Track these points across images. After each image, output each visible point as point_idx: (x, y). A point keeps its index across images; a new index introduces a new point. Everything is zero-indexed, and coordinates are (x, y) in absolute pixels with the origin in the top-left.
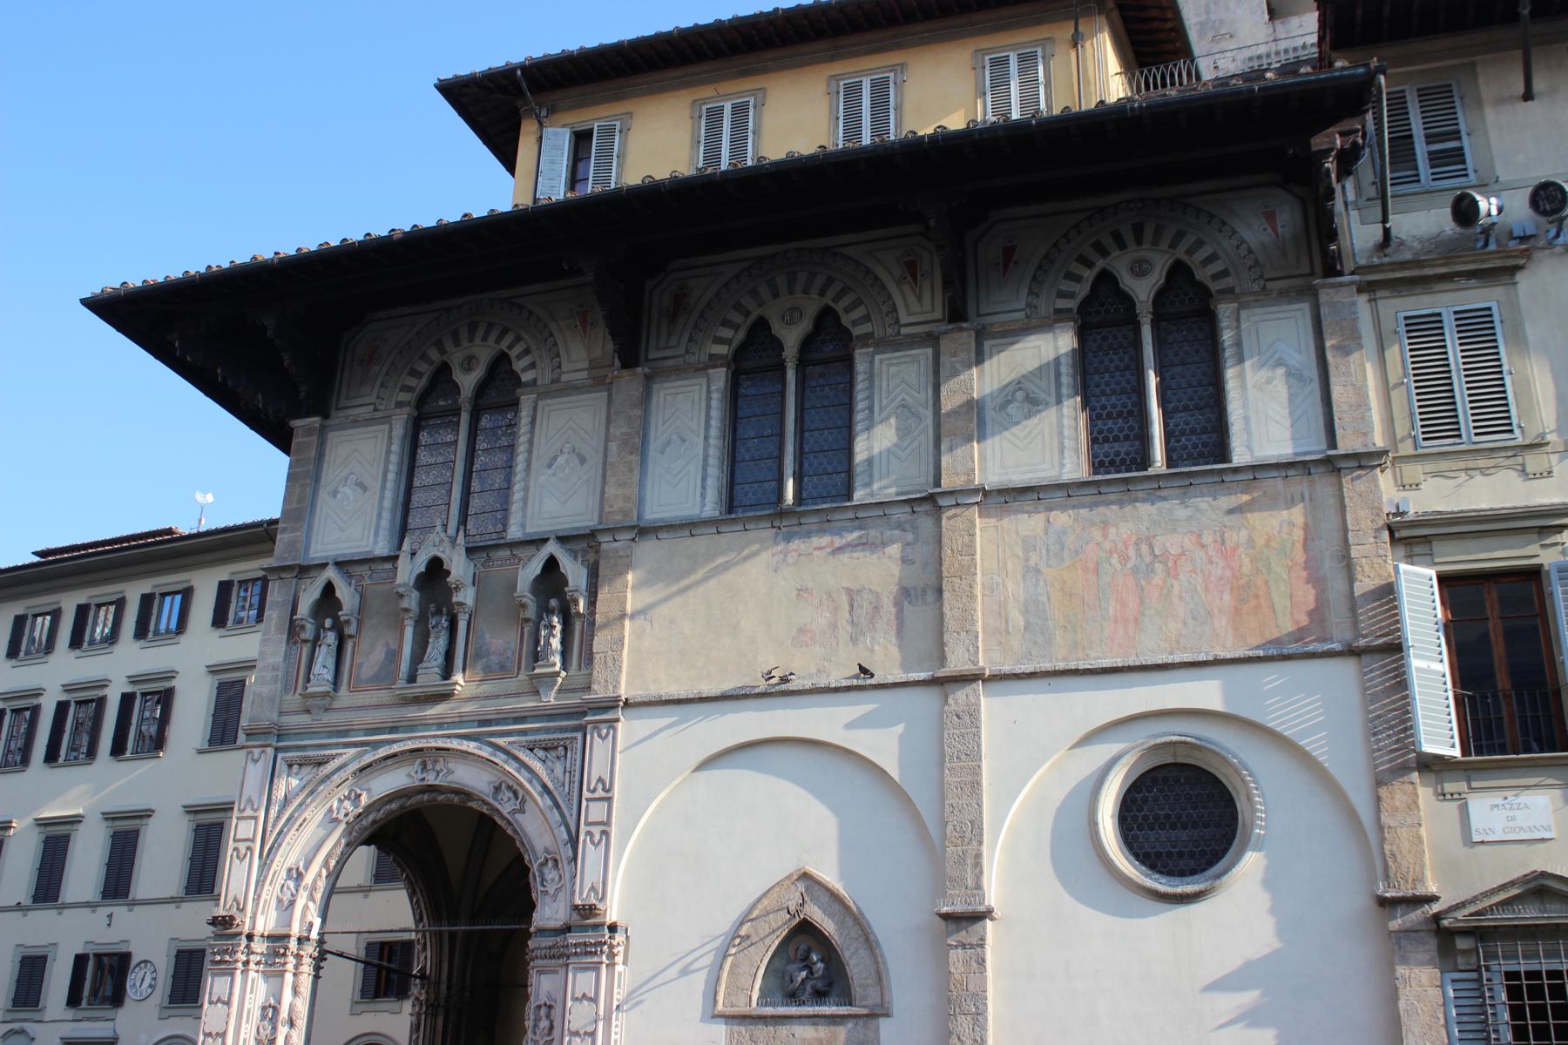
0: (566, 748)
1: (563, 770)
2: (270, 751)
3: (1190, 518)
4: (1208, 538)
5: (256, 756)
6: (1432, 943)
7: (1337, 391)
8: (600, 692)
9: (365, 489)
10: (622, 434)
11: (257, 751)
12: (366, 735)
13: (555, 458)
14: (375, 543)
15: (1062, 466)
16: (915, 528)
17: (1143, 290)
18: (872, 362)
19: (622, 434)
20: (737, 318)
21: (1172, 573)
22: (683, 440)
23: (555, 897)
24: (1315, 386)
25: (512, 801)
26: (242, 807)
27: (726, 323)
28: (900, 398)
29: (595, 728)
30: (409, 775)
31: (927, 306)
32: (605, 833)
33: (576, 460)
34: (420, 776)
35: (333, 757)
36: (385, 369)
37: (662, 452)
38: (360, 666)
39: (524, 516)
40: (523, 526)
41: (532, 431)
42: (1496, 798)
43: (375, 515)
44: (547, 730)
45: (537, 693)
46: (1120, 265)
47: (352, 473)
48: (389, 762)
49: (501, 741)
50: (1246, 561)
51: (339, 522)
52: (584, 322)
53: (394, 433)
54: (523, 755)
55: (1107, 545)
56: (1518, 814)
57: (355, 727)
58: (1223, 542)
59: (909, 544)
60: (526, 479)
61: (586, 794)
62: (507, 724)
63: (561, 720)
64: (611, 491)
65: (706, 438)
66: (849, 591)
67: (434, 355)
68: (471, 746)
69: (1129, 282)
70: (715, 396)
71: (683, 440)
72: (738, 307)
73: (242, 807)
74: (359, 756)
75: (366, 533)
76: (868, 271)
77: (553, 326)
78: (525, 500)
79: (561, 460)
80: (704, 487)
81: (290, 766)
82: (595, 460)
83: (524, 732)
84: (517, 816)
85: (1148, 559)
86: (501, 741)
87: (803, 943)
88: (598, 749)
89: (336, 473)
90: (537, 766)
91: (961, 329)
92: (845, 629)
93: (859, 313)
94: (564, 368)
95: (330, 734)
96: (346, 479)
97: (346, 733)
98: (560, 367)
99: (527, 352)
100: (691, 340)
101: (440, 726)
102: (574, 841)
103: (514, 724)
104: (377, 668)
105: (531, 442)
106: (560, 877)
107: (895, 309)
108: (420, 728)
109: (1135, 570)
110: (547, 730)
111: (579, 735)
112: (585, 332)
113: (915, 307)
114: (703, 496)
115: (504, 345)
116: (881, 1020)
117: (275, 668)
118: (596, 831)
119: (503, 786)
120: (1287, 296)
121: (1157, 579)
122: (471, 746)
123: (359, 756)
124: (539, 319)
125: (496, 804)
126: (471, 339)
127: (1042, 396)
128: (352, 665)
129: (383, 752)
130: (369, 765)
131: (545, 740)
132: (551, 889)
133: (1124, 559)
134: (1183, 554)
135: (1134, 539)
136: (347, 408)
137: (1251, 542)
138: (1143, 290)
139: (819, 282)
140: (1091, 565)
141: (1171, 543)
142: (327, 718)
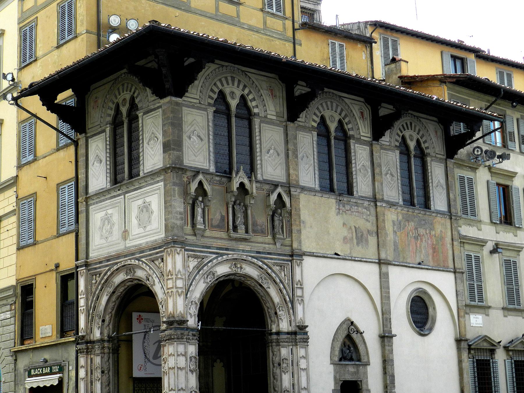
2: (183, 249)
3: (424, 224)
4: (427, 232)
6: (467, 351)
7: (451, 196)
9: (202, 140)
10: (292, 149)
11: (179, 250)
13: (269, 150)
14: (210, 166)
15: (399, 199)
16: (369, 210)
18: (355, 146)
19: (292, 149)
21: (422, 241)
22: (308, 157)
23: (282, 320)
24: (445, 191)
25: (267, 284)
28: (362, 163)
30: (230, 268)
31: (367, 132)
32: (302, 300)
33: (276, 154)
34: (234, 269)
35: (207, 257)
36: (201, 84)
37: (302, 160)
38: (212, 219)
39: (262, 171)
40: (262, 175)
41: (260, 135)
43: (207, 153)
44: (279, 259)
45: (275, 244)
47: (195, 130)
49: (266, 261)
50: (434, 240)
51: (194, 152)
52: (272, 94)
53: (209, 117)
55: (409, 228)
56: (478, 320)
57: (214, 246)
58: (430, 234)
59: (368, 215)
60: (261, 156)
61: (296, 286)
65: (314, 158)
66: (355, 227)
67: (220, 87)
70: (315, 142)
71: (308, 157)
73: (176, 273)
74: (217, 258)
75: (205, 160)
76: (351, 111)
77: (261, 91)
78: (261, 164)
79: (271, 151)
80: (315, 178)
82: (283, 155)
83: (271, 259)
85: (417, 235)
86: (266, 261)
88: (297, 270)
89: (189, 127)
90: (278, 273)
91: (378, 144)
92: (355, 241)
94: (269, 112)
95: (203, 247)
96: (193, 132)
97: (209, 247)
98: (266, 111)
100: (306, 117)
102: (292, 302)
104: (218, 222)
105: (260, 140)
107: (359, 129)
109: (415, 237)
110: (279, 259)
112: (273, 98)
113: (364, 131)
114: (315, 181)
115: (246, 91)
116: (368, 366)
117: (181, 213)
118: (300, 299)
121: (419, 242)
123: (217, 258)
124: (256, 86)
125: (262, 284)
126: (233, 84)
127: (394, 174)
128: (208, 219)
133: (413, 234)
134: (423, 235)
135: (414, 228)
136: (187, 97)
137: (435, 235)
140: (406, 234)
141: (422, 231)
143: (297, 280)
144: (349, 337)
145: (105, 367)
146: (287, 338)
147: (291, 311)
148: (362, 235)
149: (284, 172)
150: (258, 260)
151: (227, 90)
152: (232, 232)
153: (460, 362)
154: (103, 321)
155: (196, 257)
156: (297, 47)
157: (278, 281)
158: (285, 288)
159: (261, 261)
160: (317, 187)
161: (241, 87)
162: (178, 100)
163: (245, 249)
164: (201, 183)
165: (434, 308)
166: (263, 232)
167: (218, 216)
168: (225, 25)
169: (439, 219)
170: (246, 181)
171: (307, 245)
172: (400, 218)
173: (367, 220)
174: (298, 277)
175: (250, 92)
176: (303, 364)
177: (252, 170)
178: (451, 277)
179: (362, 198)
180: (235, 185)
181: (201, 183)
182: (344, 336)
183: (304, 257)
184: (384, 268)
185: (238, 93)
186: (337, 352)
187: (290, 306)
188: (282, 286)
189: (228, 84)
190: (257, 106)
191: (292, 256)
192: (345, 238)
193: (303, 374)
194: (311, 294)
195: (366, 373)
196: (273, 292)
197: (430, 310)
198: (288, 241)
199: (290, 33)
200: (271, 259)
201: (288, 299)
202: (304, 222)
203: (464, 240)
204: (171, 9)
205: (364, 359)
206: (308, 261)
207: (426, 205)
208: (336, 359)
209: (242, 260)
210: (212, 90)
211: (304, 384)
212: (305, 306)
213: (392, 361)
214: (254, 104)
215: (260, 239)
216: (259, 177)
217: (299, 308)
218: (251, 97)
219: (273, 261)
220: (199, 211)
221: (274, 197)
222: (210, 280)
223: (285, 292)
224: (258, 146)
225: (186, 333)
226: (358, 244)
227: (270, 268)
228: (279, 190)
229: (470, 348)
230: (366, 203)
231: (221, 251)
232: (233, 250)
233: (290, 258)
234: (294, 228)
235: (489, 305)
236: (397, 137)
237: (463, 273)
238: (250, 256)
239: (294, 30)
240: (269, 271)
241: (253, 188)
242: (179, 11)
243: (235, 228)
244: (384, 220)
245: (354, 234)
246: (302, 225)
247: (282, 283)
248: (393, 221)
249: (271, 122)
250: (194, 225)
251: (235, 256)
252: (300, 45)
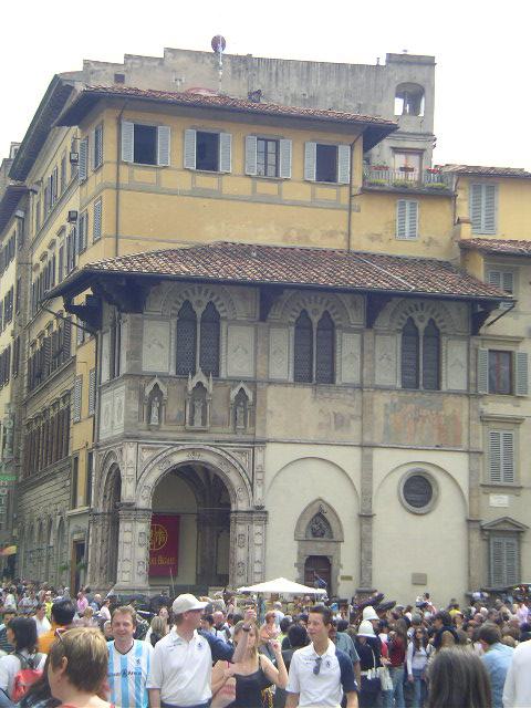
8: (259, 435)
9: (162, 347)
17: (421, 326)
20: (297, 308)
21: (424, 421)
27: (294, 310)
35: (158, 448)
42: (495, 496)
46: (415, 316)
54: (235, 455)
64: (259, 366)
69: (418, 323)
72: (298, 304)
82: (251, 353)
87: (318, 519)
88: (259, 456)
92: (333, 425)
93: (337, 316)
95: (159, 439)
97: (165, 440)
99: (222, 305)
102: (252, 485)
115: (214, 298)
120: (462, 338)
126: (200, 293)
129: (181, 447)
138: (421, 326)
139: (325, 301)
141: (425, 412)
144: (320, 515)
145: (105, 537)
147: (250, 493)
148: (342, 421)
149: (252, 368)
151: (193, 300)
152: (187, 425)
153: (469, 542)
154: (105, 496)
155: (149, 449)
156: (354, 214)
160: (291, 380)
161: (209, 295)
162: (139, 316)
164: (157, 385)
165: (438, 489)
166: (223, 424)
167: (175, 412)
168: (264, 206)
169: (451, 398)
170: (204, 381)
171: (272, 433)
172: (396, 400)
173: (350, 406)
174: (258, 461)
175: (218, 299)
176: (258, 540)
177: (213, 369)
178: (464, 457)
179: (347, 386)
180: (192, 384)
181: (157, 385)
182: (315, 512)
183: (269, 445)
184: (367, 451)
185: (205, 301)
186: (303, 530)
188: (241, 470)
189: (194, 294)
190: (225, 311)
192: (320, 424)
193: (258, 549)
194: (277, 475)
195: (338, 549)
196: (233, 477)
197: (434, 490)
198: (250, 430)
199: (345, 200)
201: (247, 481)
202: (271, 412)
203: (485, 419)
204: (199, 200)
205: (336, 538)
206: (270, 447)
207: (435, 384)
208: (302, 536)
210: (177, 302)
211: (258, 556)
212: (267, 487)
213: (370, 538)
214: (222, 308)
215: (219, 429)
216: (223, 375)
217: (258, 490)
218: (219, 303)
220: (155, 410)
221: (235, 392)
222: (165, 467)
223: (244, 475)
224: (224, 347)
225: (134, 513)
226: (336, 429)
228: (242, 385)
229: (482, 530)
230: (350, 391)
234: (258, 418)
235: (522, 484)
236: (401, 321)
237: (481, 453)
239: (351, 196)
240: (228, 457)
241: (209, 385)
242: (209, 200)
243: (192, 423)
244: (372, 406)
245: (333, 420)
246: (268, 415)
248: (386, 405)
249: (240, 323)
250: (149, 420)
252: (359, 211)
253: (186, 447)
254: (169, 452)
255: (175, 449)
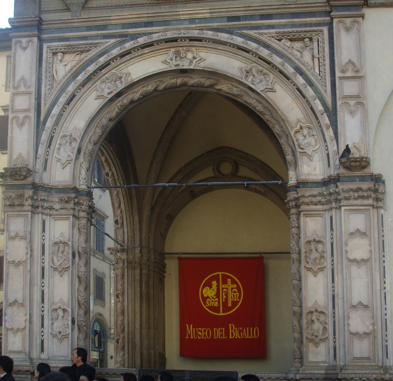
0: (311, 39)
1: (311, 57)
5: (24, 45)
12: (122, 29)
23: (310, 157)
26: (16, 85)
29: (340, 22)
30: (165, 62)
35: (96, 45)
44: (293, 25)
48: (146, 50)
54: (275, 44)
57: (113, 22)
61: (338, 74)
62: (254, 20)
63: (305, 17)
68: (224, 37)
73: (16, 85)
81: (55, 54)
84: (269, 94)
95: (89, 28)
97: (105, 27)
101: (192, 21)
102: (332, 114)
103: (261, 19)
106: (316, 141)
108: (173, 22)
110: (293, 25)
111: (325, 30)
119: (254, 70)
122: (224, 37)
123: (122, 43)
129: (142, 41)
130: (128, 52)
131: (293, 32)
132: (309, 151)
142: (85, 15)
143: (345, 61)
146: (321, 194)
147: (329, 134)
150: (231, 33)
157: (289, 70)
158: (310, 83)
159: (242, 36)
163: (195, 16)
183: (366, 11)
187: (325, 120)
188: (300, 80)
191: (328, 13)
200: (272, 27)
201: (319, 107)
209: (192, 39)
219: (273, 31)
223: (309, 92)
227: (267, 46)
231: (131, 31)
232: (165, 23)
233: (328, 19)
238: (208, 30)
240: (265, 53)
247: (301, 73)
251: (170, 35)
253: (155, 37)
254: (115, 52)
255: (128, 45)
